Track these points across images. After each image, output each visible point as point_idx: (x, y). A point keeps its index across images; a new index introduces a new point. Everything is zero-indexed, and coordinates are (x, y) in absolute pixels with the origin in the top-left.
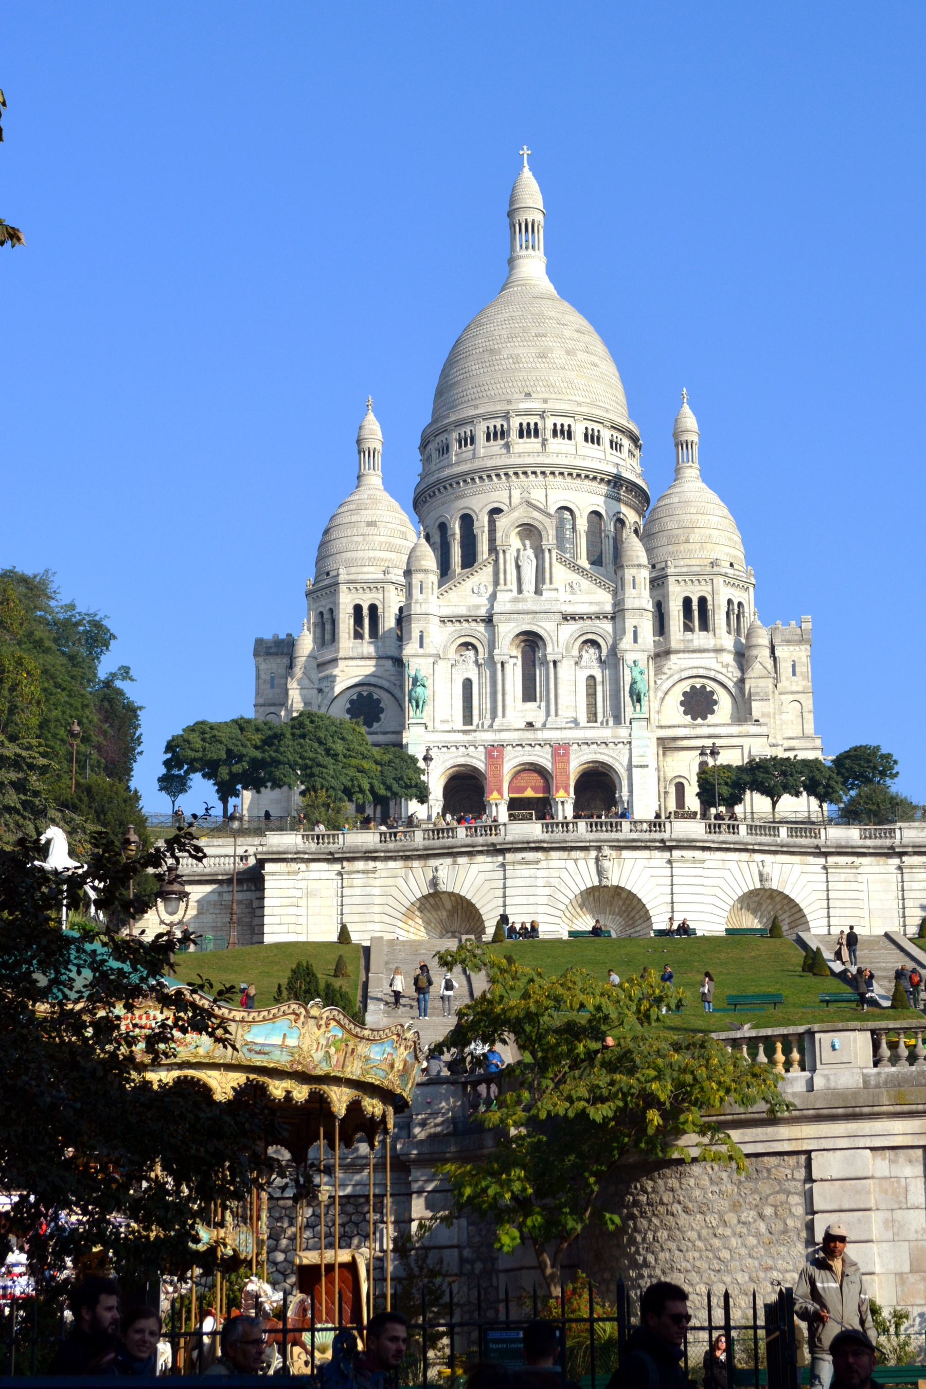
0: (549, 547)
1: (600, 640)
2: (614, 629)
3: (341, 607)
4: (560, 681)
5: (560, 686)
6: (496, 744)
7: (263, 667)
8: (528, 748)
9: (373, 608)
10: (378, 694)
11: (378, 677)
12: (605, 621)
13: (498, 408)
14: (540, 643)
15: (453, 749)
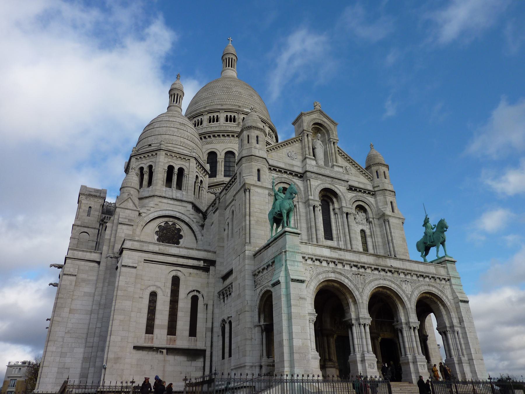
0: (335, 141)
1: (367, 207)
2: (376, 201)
3: (160, 164)
4: (351, 228)
5: (351, 232)
6: (359, 265)
7: (84, 201)
8: (383, 273)
9: (181, 171)
10: (179, 225)
11: (183, 214)
12: (369, 195)
13: (234, 108)
14: (335, 200)
15: (324, 264)
